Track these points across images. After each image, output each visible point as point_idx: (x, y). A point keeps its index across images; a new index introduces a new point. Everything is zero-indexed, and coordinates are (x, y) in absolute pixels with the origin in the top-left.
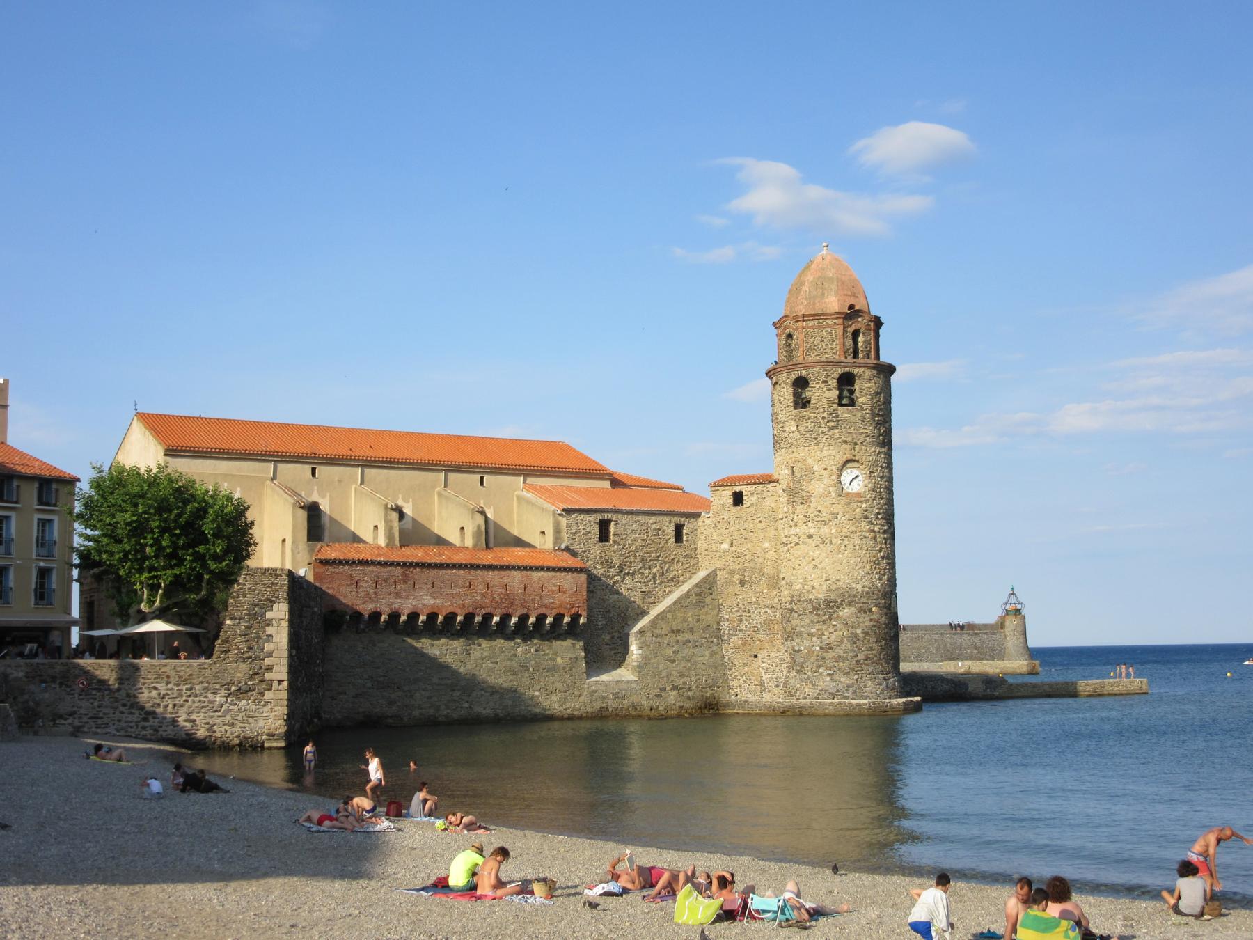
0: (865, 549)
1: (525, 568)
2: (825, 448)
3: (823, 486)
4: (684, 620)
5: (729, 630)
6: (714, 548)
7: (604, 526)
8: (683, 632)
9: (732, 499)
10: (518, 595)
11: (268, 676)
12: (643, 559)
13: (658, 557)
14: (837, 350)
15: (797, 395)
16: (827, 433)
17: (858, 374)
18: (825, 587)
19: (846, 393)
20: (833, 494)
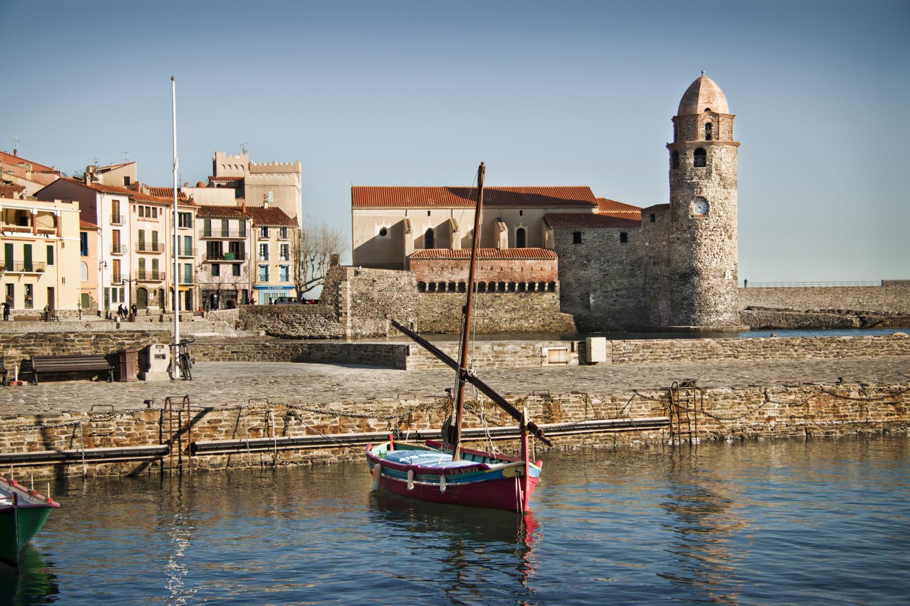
6: (642, 245)
10: (518, 272)
11: (340, 311)
12: (599, 251)
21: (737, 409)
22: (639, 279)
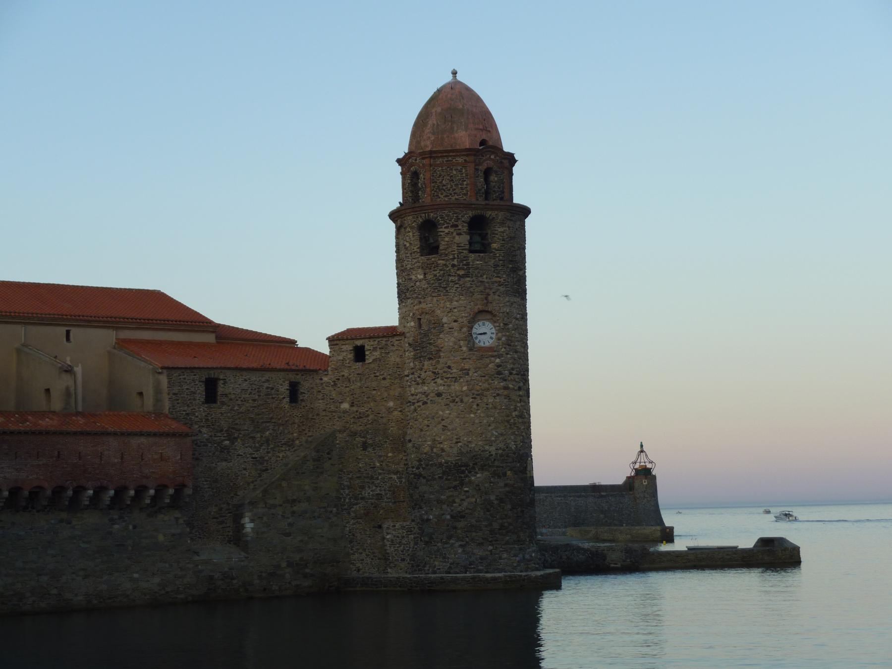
0: (499, 407)
1: (122, 434)
2: (456, 299)
3: (453, 339)
5: (350, 499)
6: (333, 408)
7: (211, 386)
8: (300, 502)
9: (352, 355)
12: (252, 420)
13: (272, 418)
14: (467, 191)
15: (424, 239)
16: (457, 282)
17: (491, 218)
18: (455, 450)
19: (477, 238)
20: (464, 349)
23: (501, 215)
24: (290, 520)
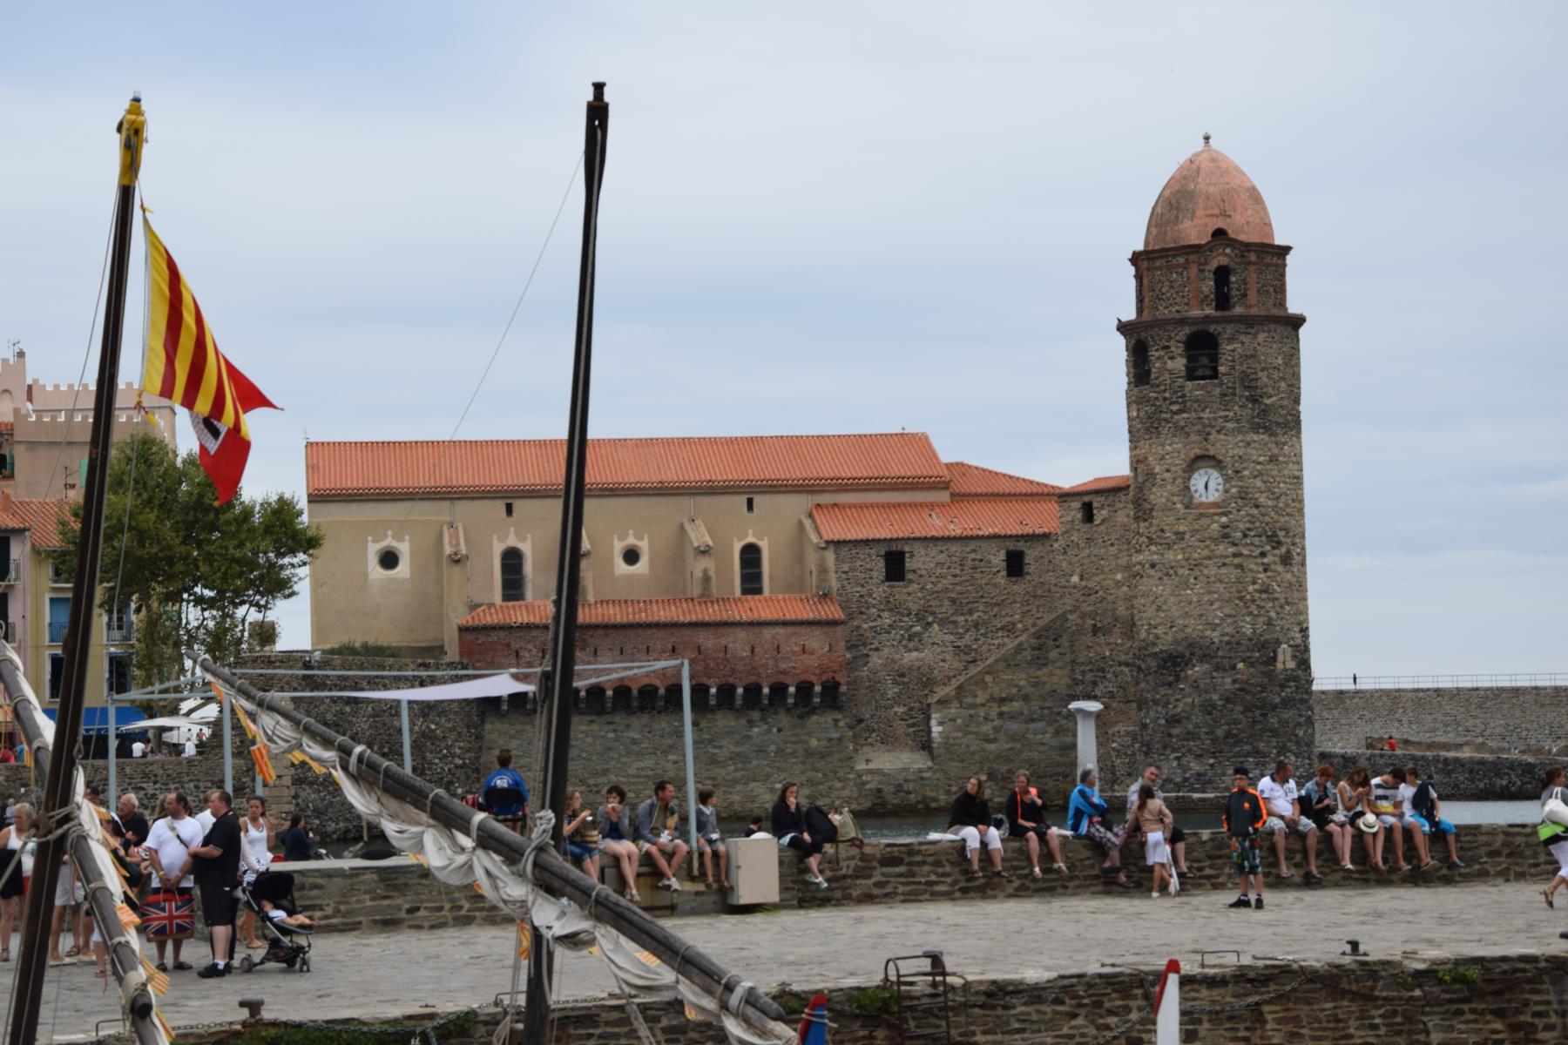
4: (1011, 684)
6: (1063, 582)
8: (1012, 701)
10: (742, 658)
12: (953, 601)
13: (982, 597)
18: (1169, 638)
20: (1179, 506)
21: (1065, 1030)
22: (1059, 672)
23: (1230, 329)
24: (995, 723)
